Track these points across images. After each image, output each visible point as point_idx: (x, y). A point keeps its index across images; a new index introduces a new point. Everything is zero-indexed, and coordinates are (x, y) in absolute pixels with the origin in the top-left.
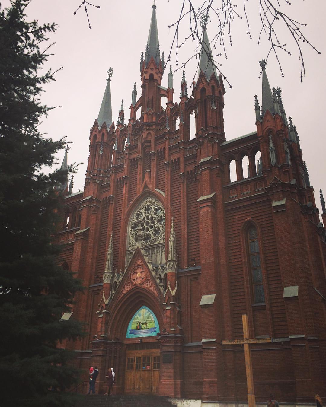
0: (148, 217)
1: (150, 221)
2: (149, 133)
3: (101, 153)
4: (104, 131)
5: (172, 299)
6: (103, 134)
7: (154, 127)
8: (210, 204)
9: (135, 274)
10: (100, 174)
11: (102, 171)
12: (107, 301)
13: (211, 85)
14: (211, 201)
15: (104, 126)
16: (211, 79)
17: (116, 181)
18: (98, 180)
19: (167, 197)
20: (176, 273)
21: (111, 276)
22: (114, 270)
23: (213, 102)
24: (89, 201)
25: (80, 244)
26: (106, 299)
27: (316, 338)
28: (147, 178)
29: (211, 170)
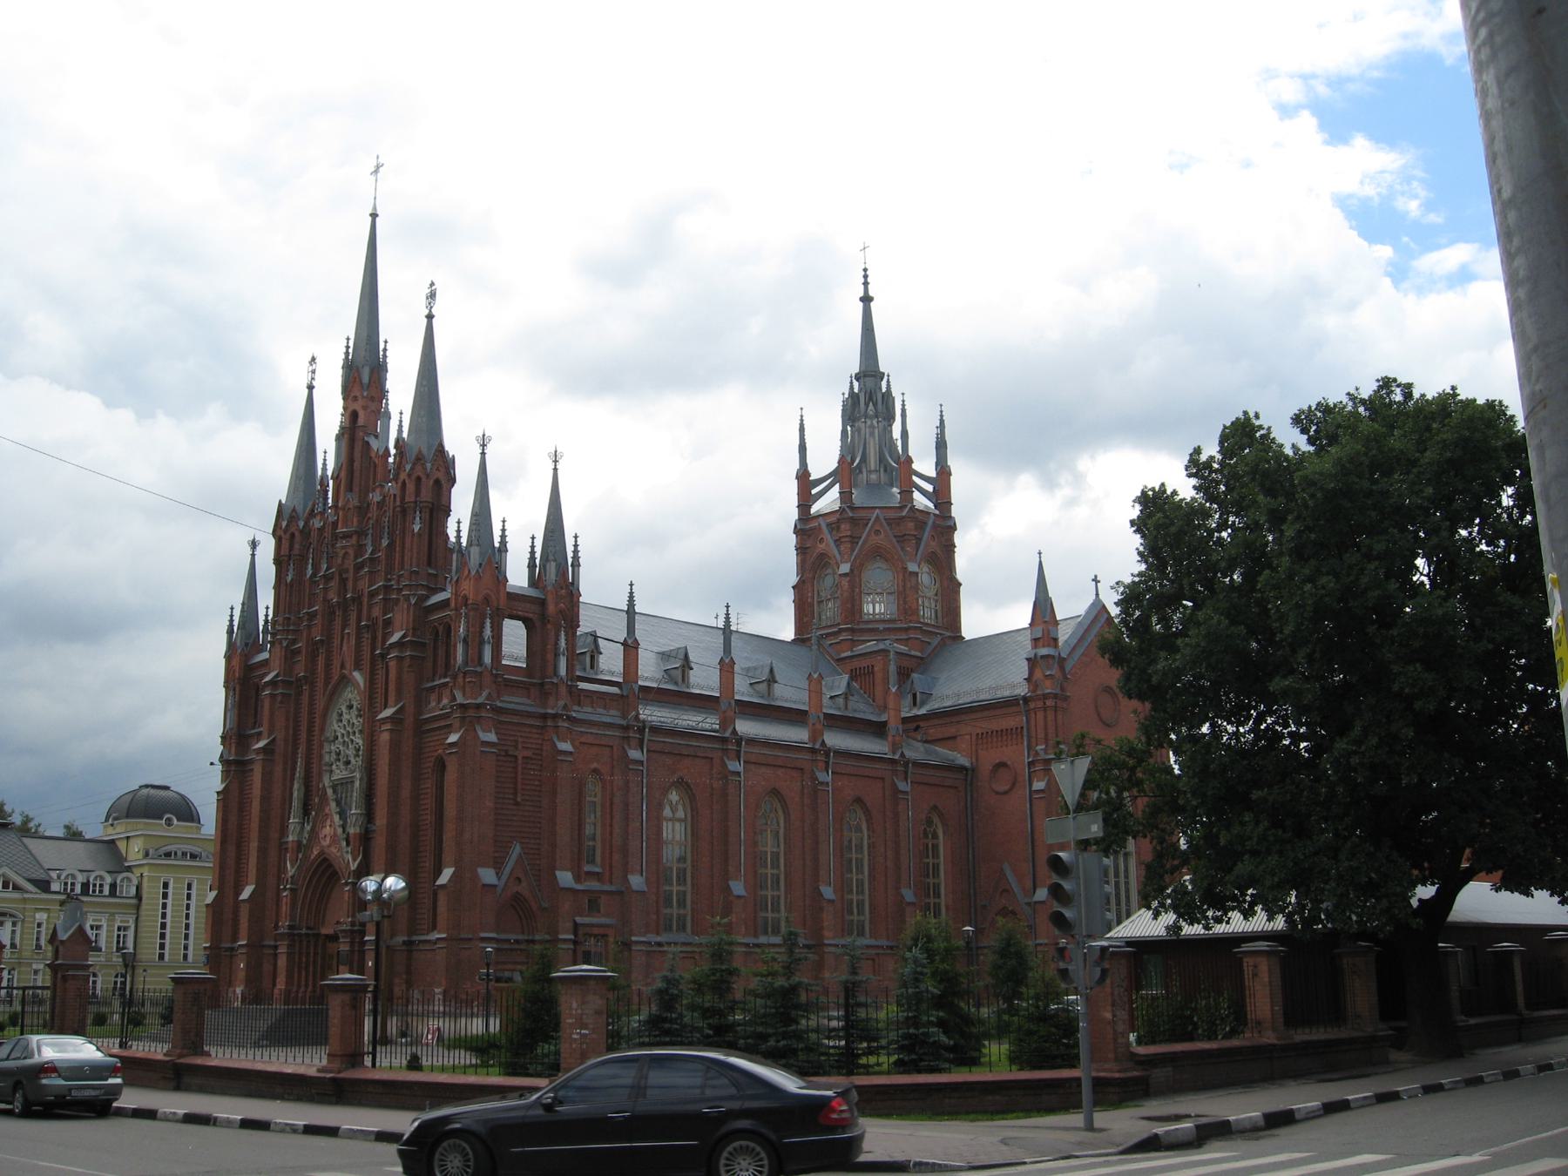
0: (349, 721)
1: (351, 731)
2: (346, 553)
3: (289, 579)
4: (293, 529)
5: (352, 874)
6: (293, 535)
7: (355, 538)
8: (388, 726)
9: (324, 829)
10: (288, 625)
11: (292, 618)
12: (293, 870)
13: (413, 477)
14: (392, 722)
15: (294, 517)
16: (414, 464)
17: (310, 642)
18: (286, 639)
19: (365, 692)
20: (363, 832)
21: (298, 829)
22: (304, 819)
23: (418, 513)
24: (273, 683)
25: (261, 770)
26: (292, 866)
27: (470, 936)
28: (345, 648)
29: (400, 659)
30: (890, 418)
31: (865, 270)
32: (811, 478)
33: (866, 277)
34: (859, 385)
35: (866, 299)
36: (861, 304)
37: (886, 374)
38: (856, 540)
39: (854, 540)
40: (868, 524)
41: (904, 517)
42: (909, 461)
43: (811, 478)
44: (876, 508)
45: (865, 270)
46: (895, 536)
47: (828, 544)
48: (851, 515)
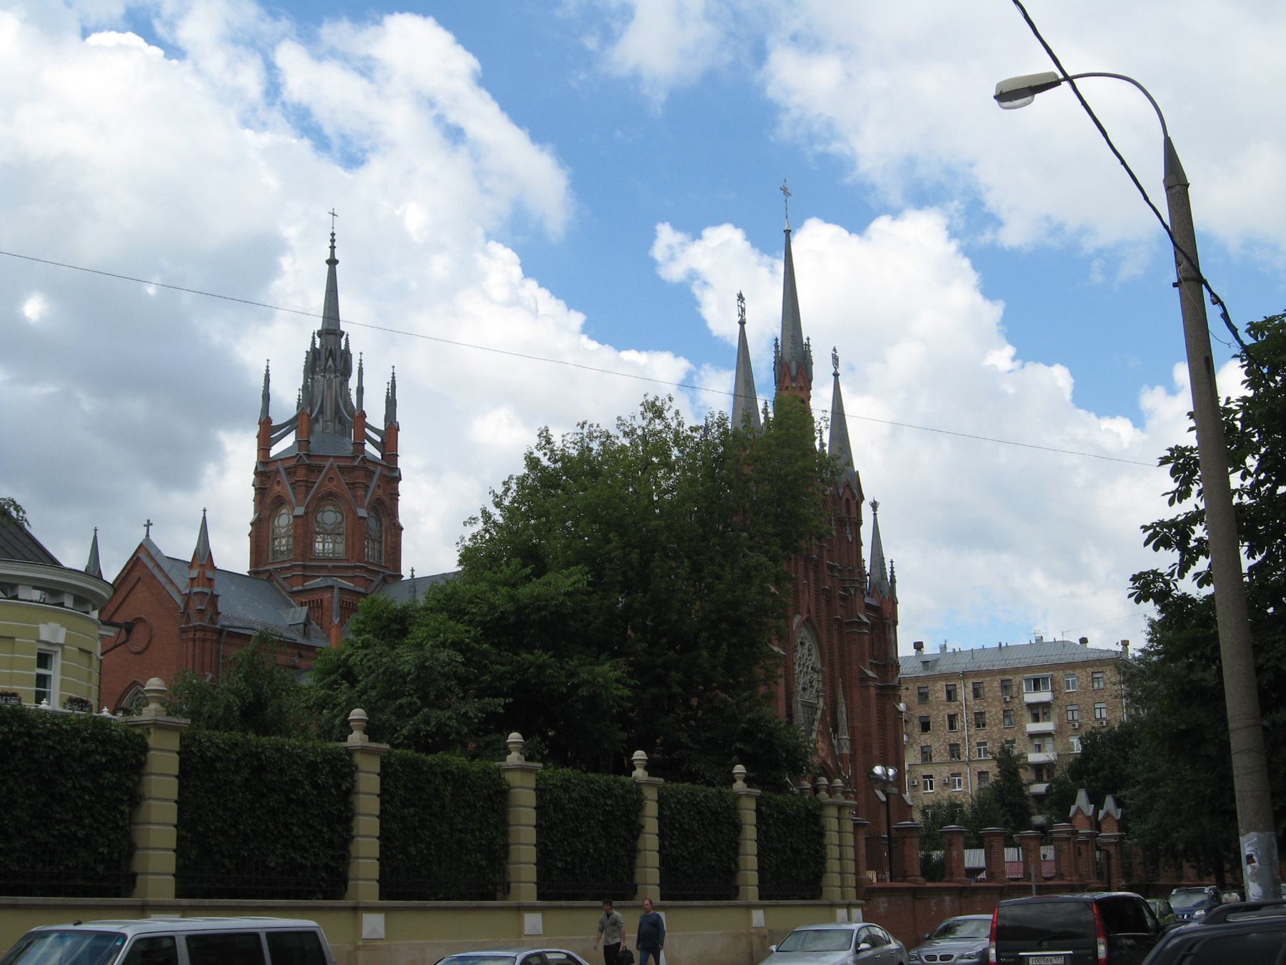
30: (347, 373)
31: (333, 234)
33: (333, 241)
34: (321, 342)
35: (332, 262)
36: (327, 266)
37: (346, 333)
38: (309, 485)
39: (308, 485)
40: (320, 472)
41: (355, 467)
42: (363, 415)
44: (329, 457)
45: (333, 234)
46: (347, 483)
47: (284, 487)
48: (308, 462)
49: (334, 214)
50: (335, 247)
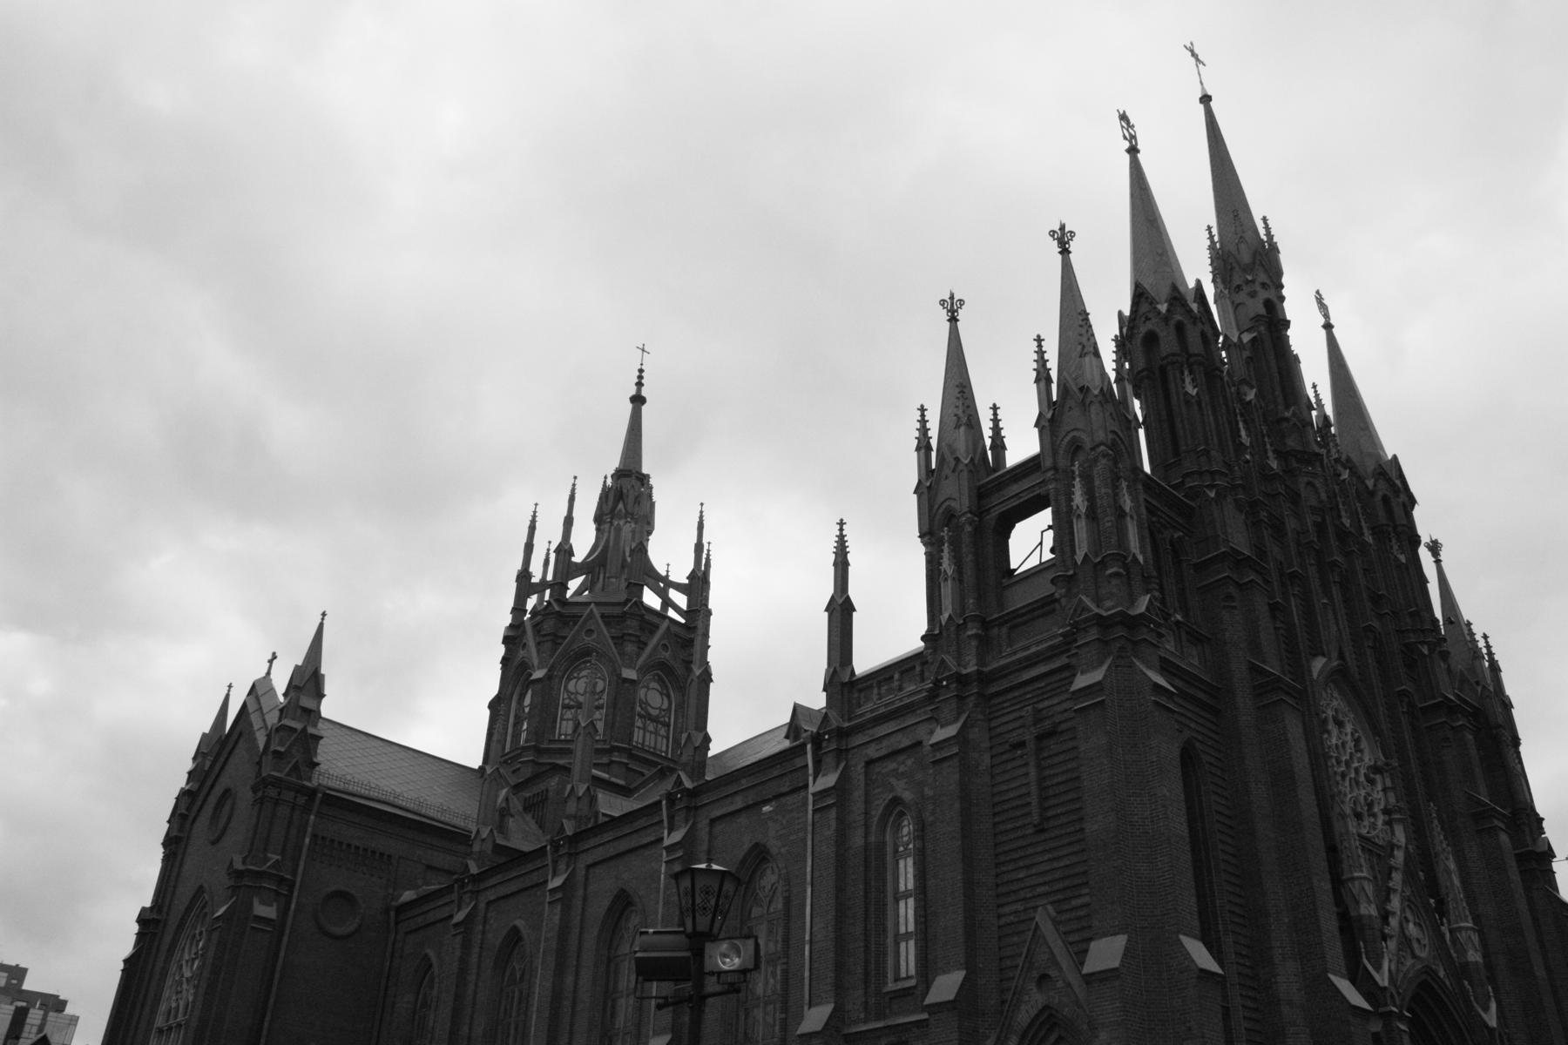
31: (641, 371)
32: (573, 559)
33: (640, 377)
35: (638, 400)
38: (641, 646)
43: (573, 559)
45: (641, 371)
49: (643, 350)
50: (643, 385)
